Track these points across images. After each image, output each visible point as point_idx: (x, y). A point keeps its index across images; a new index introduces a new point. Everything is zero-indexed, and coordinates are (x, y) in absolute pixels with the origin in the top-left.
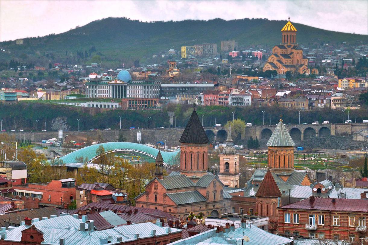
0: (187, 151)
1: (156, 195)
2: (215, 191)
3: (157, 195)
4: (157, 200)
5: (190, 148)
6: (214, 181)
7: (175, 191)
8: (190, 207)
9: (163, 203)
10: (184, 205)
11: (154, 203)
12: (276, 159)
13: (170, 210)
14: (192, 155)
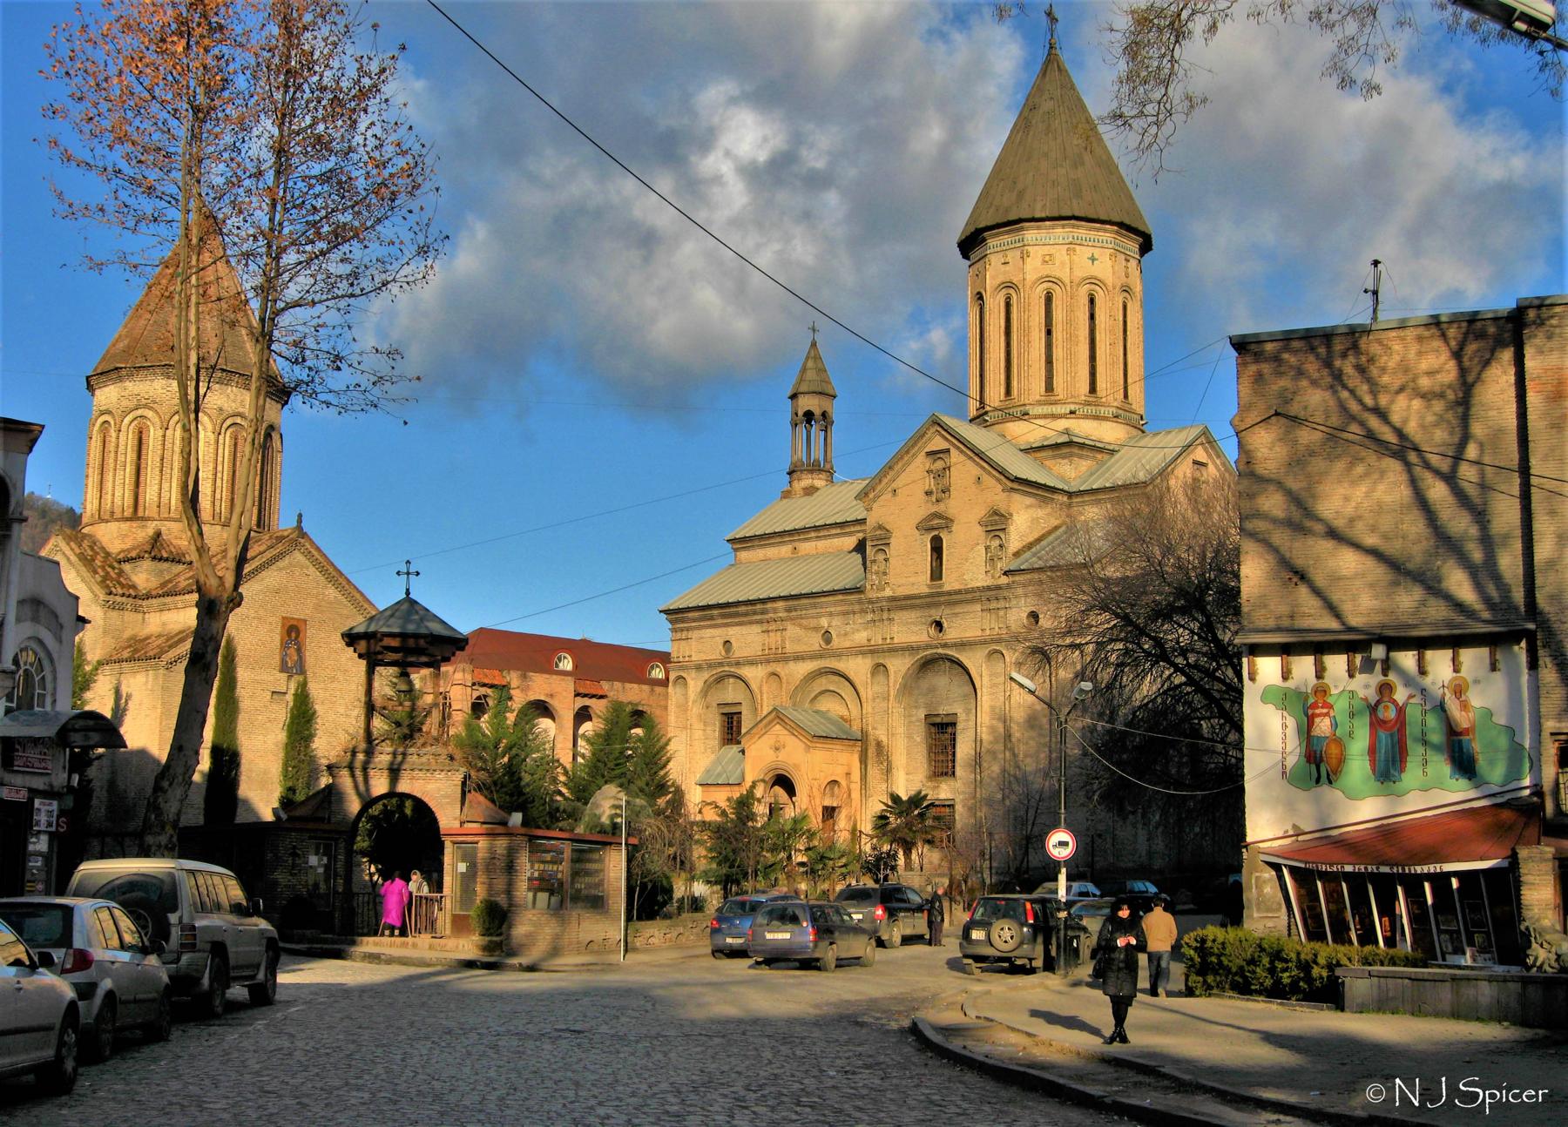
6: (929, 454)
8: (756, 629)
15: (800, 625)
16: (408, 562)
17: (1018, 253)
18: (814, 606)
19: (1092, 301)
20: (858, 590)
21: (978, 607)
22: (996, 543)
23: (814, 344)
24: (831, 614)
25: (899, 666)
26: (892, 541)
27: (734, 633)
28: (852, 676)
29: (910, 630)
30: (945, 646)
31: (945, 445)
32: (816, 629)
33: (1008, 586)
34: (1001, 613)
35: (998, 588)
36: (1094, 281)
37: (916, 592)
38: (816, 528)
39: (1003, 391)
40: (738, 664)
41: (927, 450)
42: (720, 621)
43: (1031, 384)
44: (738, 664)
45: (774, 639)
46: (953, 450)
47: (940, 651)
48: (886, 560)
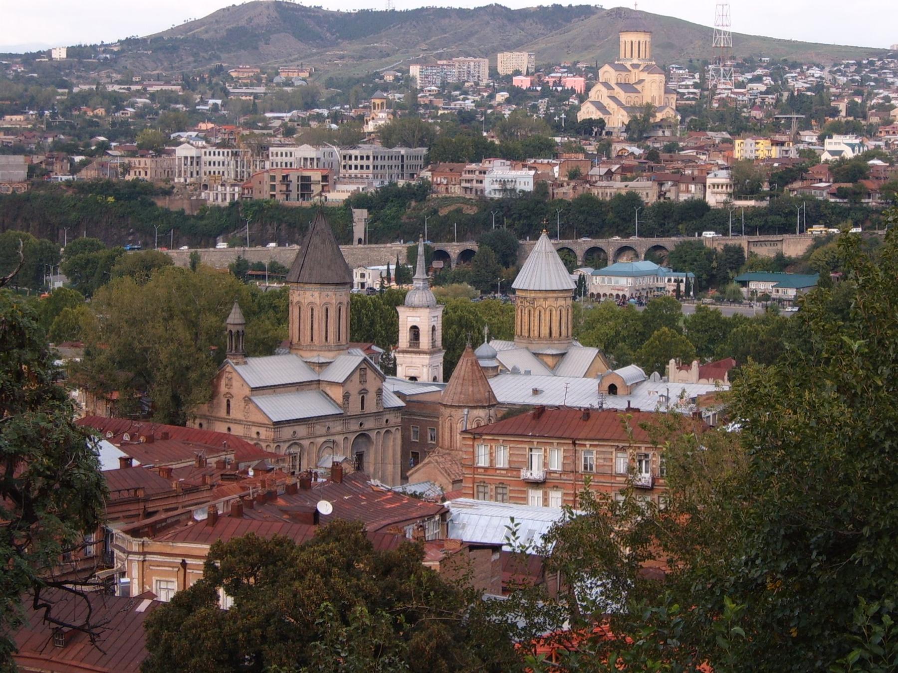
0: (303, 301)
1: (228, 401)
2: (363, 392)
3: (231, 400)
4: (231, 411)
5: (309, 293)
7: (272, 390)
8: (305, 426)
9: (243, 418)
11: (224, 418)
12: (532, 318)
13: (258, 433)
14: (312, 310)
21: (372, 418)
27: (297, 428)
31: (365, 366)
32: (325, 426)
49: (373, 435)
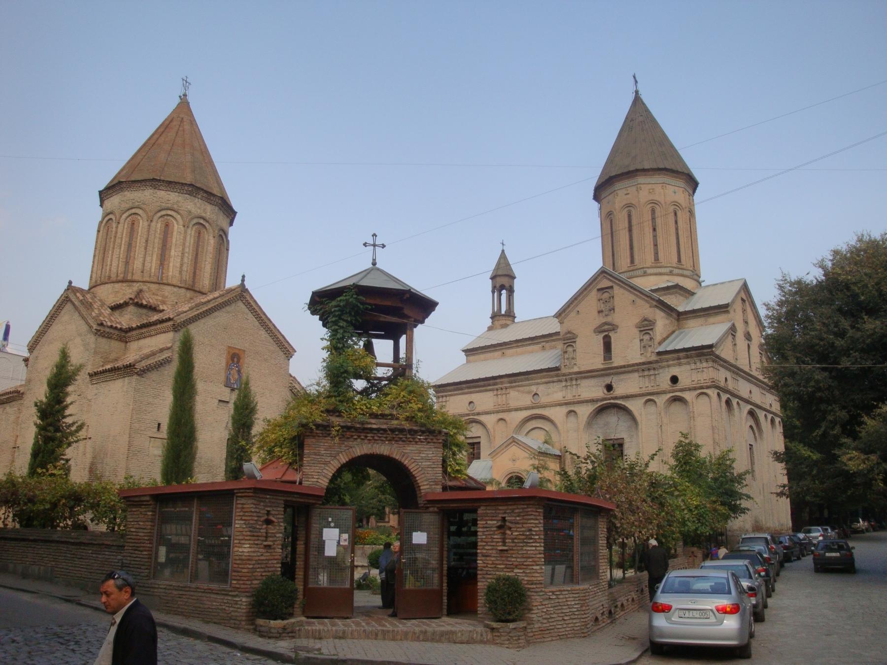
6: (599, 290)
8: (490, 394)
10: (462, 389)
15: (518, 391)
16: (374, 235)
17: (634, 189)
18: (528, 380)
19: (676, 214)
20: (557, 369)
21: (636, 375)
22: (647, 337)
23: (503, 251)
24: (538, 384)
25: (584, 411)
26: (578, 340)
27: (474, 397)
28: (552, 418)
29: (593, 390)
30: (616, 398)
31: (609, 284)
32: (529, 392)
33: (657, 362)
34: (652, 377)
35: (650, 363)
36: (676, 204)
37: (595, 368)
38: (517, 341)
39: (629, 260)
40: (478, 414)
41: (598, 287)
42: (466, 391)
43: (645, 257)
44: (478, 414)
45: (501, 400)
46: (616, 287)
47: (612, 401)
48: (574, 351)
49: (635, 406)
